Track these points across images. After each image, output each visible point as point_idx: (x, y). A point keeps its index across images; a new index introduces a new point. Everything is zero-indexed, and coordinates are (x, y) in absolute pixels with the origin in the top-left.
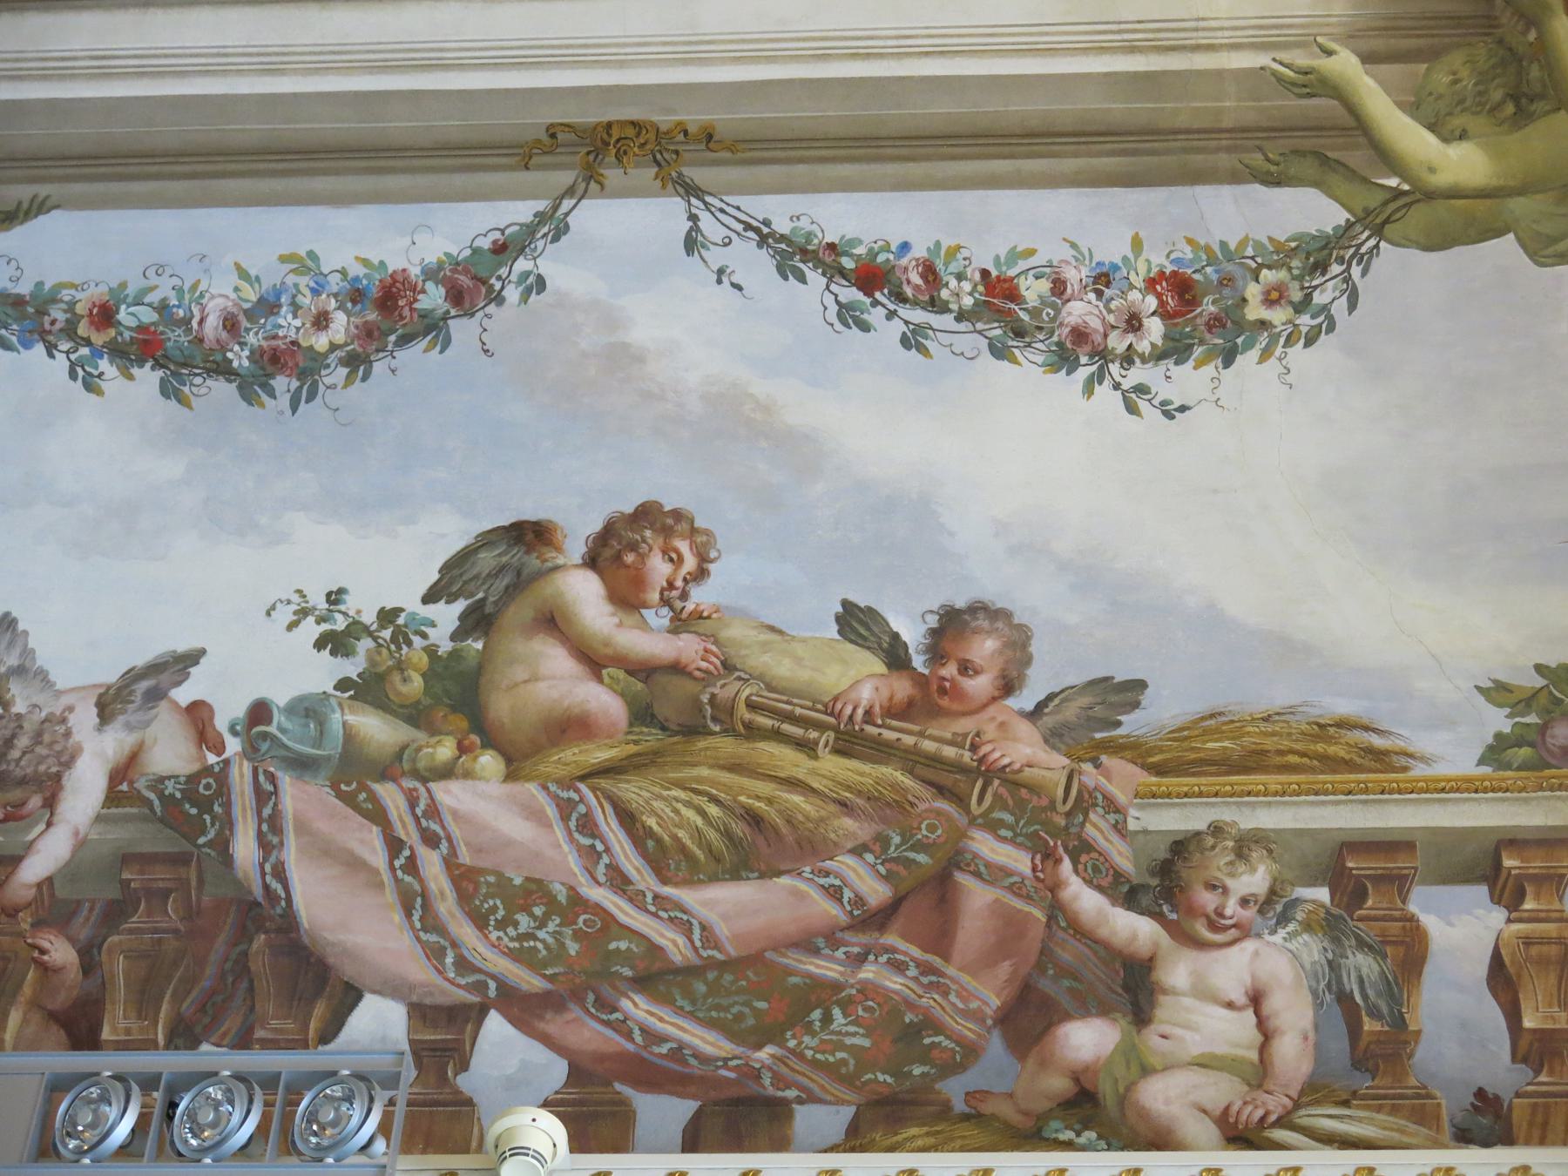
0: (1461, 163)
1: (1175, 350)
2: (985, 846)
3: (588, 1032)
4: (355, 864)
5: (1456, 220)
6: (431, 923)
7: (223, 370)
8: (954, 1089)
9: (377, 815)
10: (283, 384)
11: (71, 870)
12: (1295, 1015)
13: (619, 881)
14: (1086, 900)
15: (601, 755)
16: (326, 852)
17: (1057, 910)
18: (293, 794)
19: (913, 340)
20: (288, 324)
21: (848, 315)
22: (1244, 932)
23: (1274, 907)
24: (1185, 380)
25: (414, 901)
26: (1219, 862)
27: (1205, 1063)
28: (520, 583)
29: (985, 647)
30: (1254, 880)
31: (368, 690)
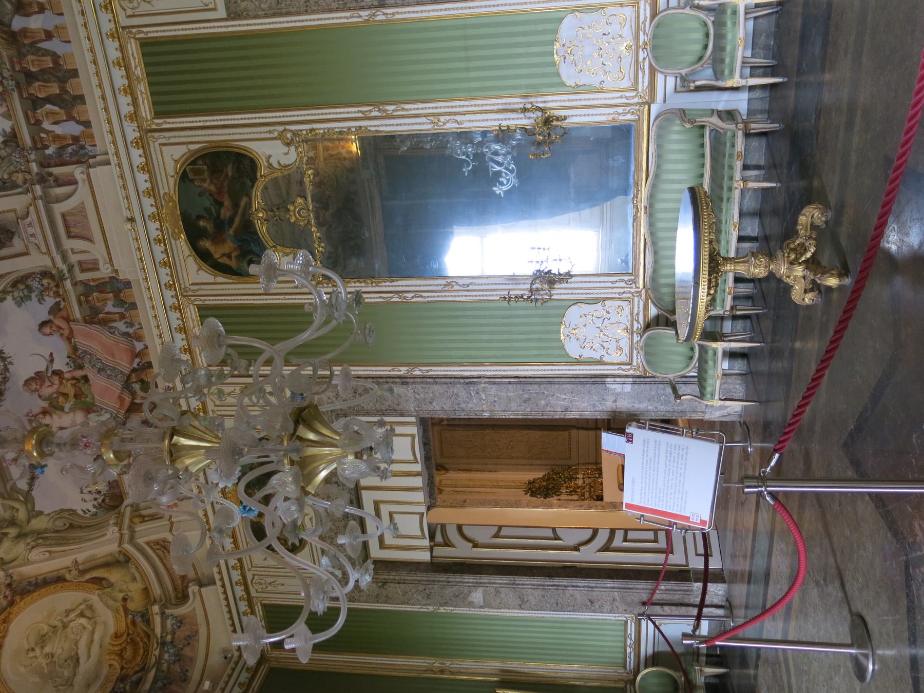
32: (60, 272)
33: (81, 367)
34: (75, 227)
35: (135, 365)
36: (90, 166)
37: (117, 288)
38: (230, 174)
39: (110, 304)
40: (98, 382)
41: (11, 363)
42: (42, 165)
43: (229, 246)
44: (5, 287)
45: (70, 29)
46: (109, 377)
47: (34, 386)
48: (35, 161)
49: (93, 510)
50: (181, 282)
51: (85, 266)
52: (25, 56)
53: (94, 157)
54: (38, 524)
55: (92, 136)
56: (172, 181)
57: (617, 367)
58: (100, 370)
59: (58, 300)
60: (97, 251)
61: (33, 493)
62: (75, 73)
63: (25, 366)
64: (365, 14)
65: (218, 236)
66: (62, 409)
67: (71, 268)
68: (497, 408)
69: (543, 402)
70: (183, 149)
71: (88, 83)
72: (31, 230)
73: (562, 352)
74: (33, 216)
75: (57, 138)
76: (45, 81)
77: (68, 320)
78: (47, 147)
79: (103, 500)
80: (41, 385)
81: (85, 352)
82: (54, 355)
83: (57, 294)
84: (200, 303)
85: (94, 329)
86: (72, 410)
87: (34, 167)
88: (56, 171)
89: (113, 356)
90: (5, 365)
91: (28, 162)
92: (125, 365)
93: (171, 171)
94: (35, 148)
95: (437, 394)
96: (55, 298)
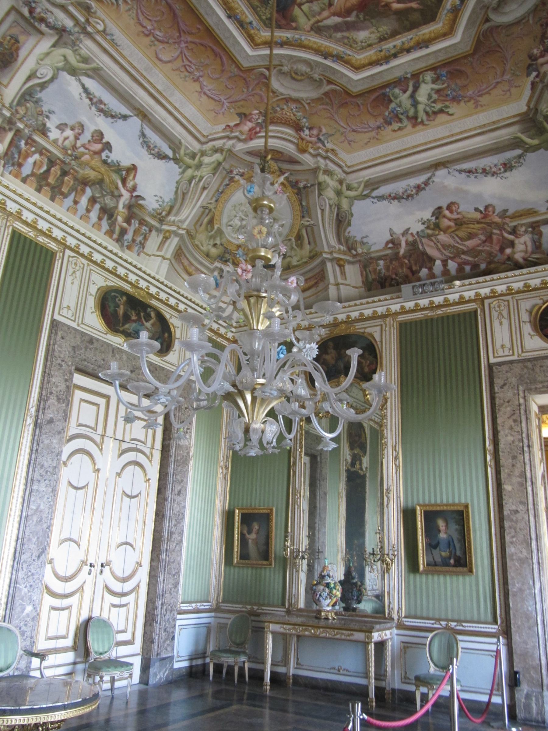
0: (535, 142)
1: (505, 171)
2: (495, 231)
3: (459, 260)
4: (431, 246)
5: (534, 149)
6: (441, 251)
7: (403, 198)
8: (496, 259)
9: (432, 241)
10: (410, 198)
11: (405, 252)
12: (529, 244)
13: (458, 243)
14: (506, 235)
15: (453, 230)
16: (428, 246)
17: (503, 237)
18: (424, 240)
19: (476, 177)
20: (409, 192)
21: (468, 176)
22: (523, 235)
23: (526, 232)
24: (507, 174)
25: (438, 249)
26: (519, 228)
27: (520, 252)
28: (440, 213)
29: (490, 209)
30: (523, 229)
31: (428, 228)
42: (18, 132)
45: (72, 215)
48: (23, 130)
52: (74, 181)
55: (16, 176)
62: (53, 199)
64: (33, 411)
71: (42, 200)
76: (58, 179)
78: (26, 144)
87: (21, 126)
91: (26, 125)
94: (30, 138)
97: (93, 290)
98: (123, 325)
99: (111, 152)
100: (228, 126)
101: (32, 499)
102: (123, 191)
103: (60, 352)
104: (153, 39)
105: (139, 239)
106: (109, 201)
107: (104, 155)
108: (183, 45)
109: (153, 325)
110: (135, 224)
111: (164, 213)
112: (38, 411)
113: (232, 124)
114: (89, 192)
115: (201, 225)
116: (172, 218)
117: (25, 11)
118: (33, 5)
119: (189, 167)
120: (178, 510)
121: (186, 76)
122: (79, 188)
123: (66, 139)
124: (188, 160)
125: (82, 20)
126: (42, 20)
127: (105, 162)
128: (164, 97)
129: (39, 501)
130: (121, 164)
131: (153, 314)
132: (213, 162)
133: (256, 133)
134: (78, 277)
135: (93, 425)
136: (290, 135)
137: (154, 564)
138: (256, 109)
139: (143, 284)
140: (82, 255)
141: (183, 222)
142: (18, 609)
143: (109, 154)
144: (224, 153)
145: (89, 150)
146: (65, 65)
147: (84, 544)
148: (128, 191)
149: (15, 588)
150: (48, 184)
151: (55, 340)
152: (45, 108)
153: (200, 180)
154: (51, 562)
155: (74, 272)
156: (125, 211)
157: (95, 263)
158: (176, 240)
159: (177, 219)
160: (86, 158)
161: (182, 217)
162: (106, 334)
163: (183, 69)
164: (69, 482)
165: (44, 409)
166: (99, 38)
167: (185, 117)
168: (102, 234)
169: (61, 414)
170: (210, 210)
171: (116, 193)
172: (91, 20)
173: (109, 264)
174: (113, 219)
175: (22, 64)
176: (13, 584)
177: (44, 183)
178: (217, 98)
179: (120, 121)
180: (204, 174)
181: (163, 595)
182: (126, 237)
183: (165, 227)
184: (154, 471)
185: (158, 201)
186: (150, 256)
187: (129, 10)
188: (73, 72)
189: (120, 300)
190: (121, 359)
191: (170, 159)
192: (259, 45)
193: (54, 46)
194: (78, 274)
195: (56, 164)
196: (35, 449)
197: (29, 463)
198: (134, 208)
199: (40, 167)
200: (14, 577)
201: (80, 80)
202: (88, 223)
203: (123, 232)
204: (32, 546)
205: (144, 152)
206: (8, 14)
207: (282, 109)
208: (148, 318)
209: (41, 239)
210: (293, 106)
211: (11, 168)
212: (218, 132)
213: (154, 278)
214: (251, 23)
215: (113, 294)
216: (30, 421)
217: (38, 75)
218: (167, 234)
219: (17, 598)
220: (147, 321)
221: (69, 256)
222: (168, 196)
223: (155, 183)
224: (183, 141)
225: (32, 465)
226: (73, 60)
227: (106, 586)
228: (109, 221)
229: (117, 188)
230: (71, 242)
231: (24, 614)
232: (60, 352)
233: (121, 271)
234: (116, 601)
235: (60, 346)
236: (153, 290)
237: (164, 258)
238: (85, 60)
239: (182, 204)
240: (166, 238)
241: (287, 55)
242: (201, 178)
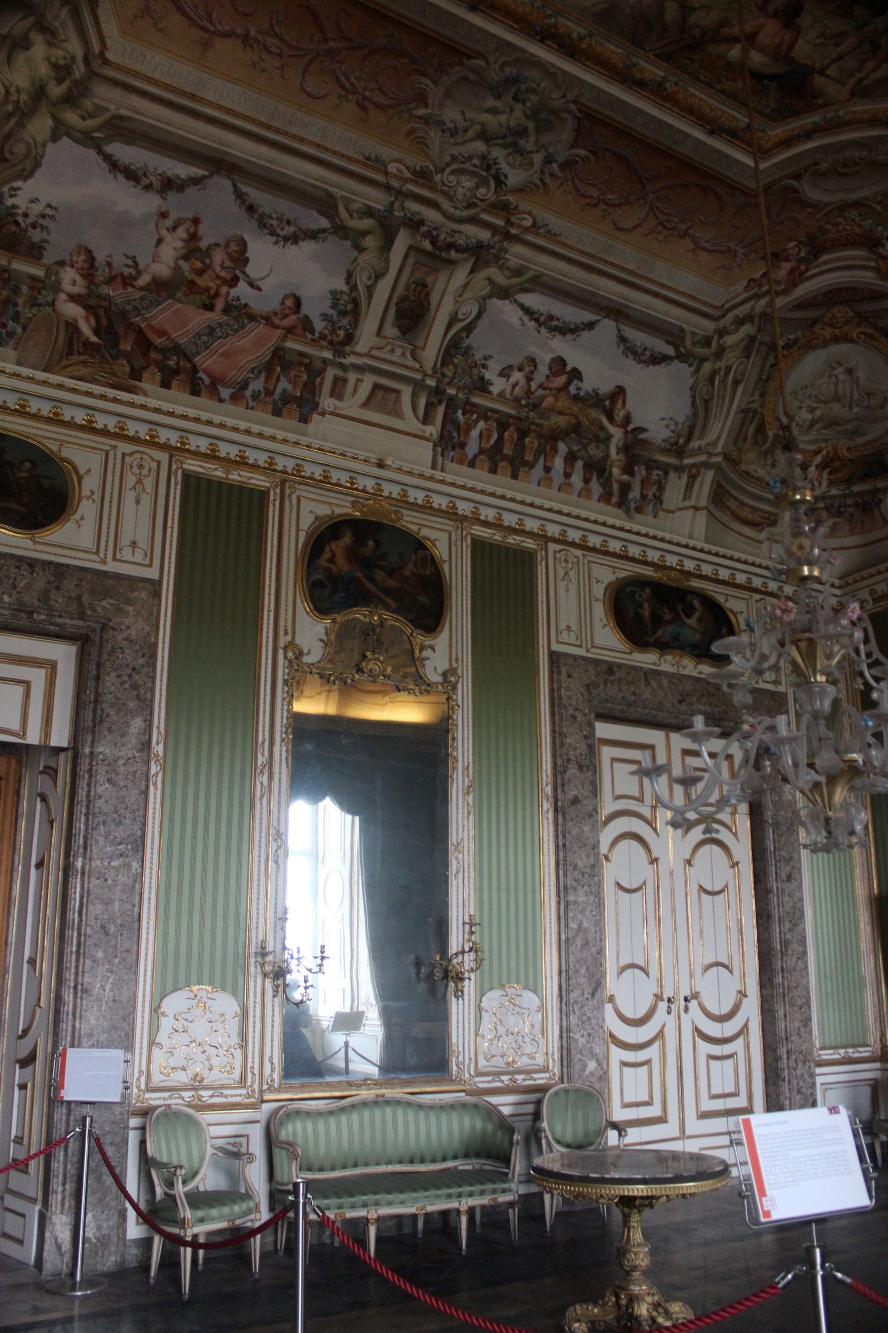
32: (345, 355)
33: (227, 310)
34: (382, 397)
35: (201, 374)
36: (435, 446)
37: (304, 406)
38: (421, 598)
39: (289, 387)
40: (199, 320)
41: (276, 243)
43: (342, 564)
44: (358, 291)
46: (198, 335)
47: (234, 247)
48: (457, 395)
49: (9, 202)
50: (302, 487)
51: (340, 383)
52: (539, 439)
53: (442, 455)
54: (40, 126)
55: (461, 462)
56: (415, 528)
57: (144, 1068)
58: (211, 330)
59: (317, 334)
60: (351, 405)
61: (92, 153)
62: (515, 476)
63: (262, 254)
64: (549, 790)
65: (352, 554)
66: (186, 258)
67: (344, 368)
68: (94, 882)
69: (100, 955)
70: (445, 557)
72: (398, 352)
73: (169, 986)
74: (410, 363)
75: (469, 428)
76: (516, 445)
77: (289, 330)
78: (464, 414)
79: (17, 224)
80: (229, 255)
81: (243, 326)
82: (256, 292)
83: (323, 337)
84: (272, 498)
85: (264, 353)
86: (177, 269)
87: (452, 391)
88: (441, 410)
89: (223, 355)
90: (278, 235)
91: (459, 389)
92: (207, 362)
93: (424, 532)
94: (467, 402)
95: (123, 792)
96: (320, 333)
97: (599, 591)
98: (654, 633)
99: (581, 380)
100: (753, 280)
101: (571, 915)
102: (612, 429)
103: (569, 697)
104: (604, 207)
105: (651, 491)
106: (594, 451)
107: (572, 389)
108: (651, 197)
109: (699, 620)
110: (641, 471)
111: (681, 441)
112: (555, 789)
113: (757, 276)
114: (562, 447)
115: (745, 439)
116: (695, 444)
117: (427, 245)
118: (435, 233)
119: (703, 360)
120: (791, 904)
121: (666, 237)
122: (548, 447)
123: (515, 386)
124: (699, 351)
125: (502, 223)
126: (450, 246)
127: (576, 398)
128: (641, 277)
129: (579, 917)
130: (601, 392)
131: (696, 604)
132: (742, 340)
133: (801, 274)
134: (573, 579)
135: (636, 794)
136: (862, 258)
137: (765, 992)
138: (790, 239)
139: (672, 560)
140: (573, 544)
141: (715, 443)
142: (578, 1066)
143: (580, 384)
144: (756, 321)
145: (550, 389)
146: (492, 290)
147: (654, 970)
148: (618, 426)
149: (569, 1038)
150: (505, 458)
151: (560, 681)
152: (478, 357)
153: (727, 373)
154: (611, 999)
155: (566, 573)
156: (622, 457)
157: (593, 550)
158: (709, 476)
159: (704, 442)
160: (549, 401)
161: (711, 436)
162: (630, 653)
163: (660, 229)
164: (618, 884)
165: (563, 785)
166: (529, 237)
167: (680, 293)
168: (593, 503)
169: (588, 787)
170: (755, 412)
171: (602, 435)
172: (513, 219)
173: (615, 546)
174: (606, 475)
175: (437, 311)
176: (565, 1033)
177: (499, 457)
178: (723, 248)
179: (585, 334)
180: (731, 361)
181: (787, 1039)
182: (631, 496)
183: (688, 461)
184: (743, 850)
185: (667, 426)
186: (674, 512)
187: (562, 184)
188: (505, 294)
189: (641, 596)
190: (660, 686)
191: (671, 358)
192: (770, 150)
193: (472, 271)
194: (572, 574)
195: (509, 425)
196: (561, 844)
197: (557, 865)
198: (635, 448)
199: (489, 437)
200: (564, 1023)
201: (516, 301)
202: (571, 493)
203: (625, 488)
204: (582, 980)
205: (630, 362)
206: (405, 259)
207: (837, 224)
208: (689, 611)
209: (512, 540)
210: (853, 214)
211: (451, 454)
212: (739, 295)
213: (686, 546)
214: (749, 127)
215: (629, 589)
216: (547, 805)
217: (460, 316)
218: (694, 471)
219: (573, 1052)
220: (689, 616)
221: (555, 552)
222: (681, 412)
223: (657, 401)
224: (685, 326)
225: (561, 867)
226: (500, 278)
227: (697, 1030)
228: (602, 480)
229: (602, 428)
230: (553, 530)
231: (587, 1073)
232: (569, 697)
233: (634, 551)
234: (716, 1050)
235: (568, 689)
236: (690, 565)
237: (696, 508)
238: (517, 272)
239: (706, 419)
240: (693, 478)
241: (821, 147)
242: (728, 369)
